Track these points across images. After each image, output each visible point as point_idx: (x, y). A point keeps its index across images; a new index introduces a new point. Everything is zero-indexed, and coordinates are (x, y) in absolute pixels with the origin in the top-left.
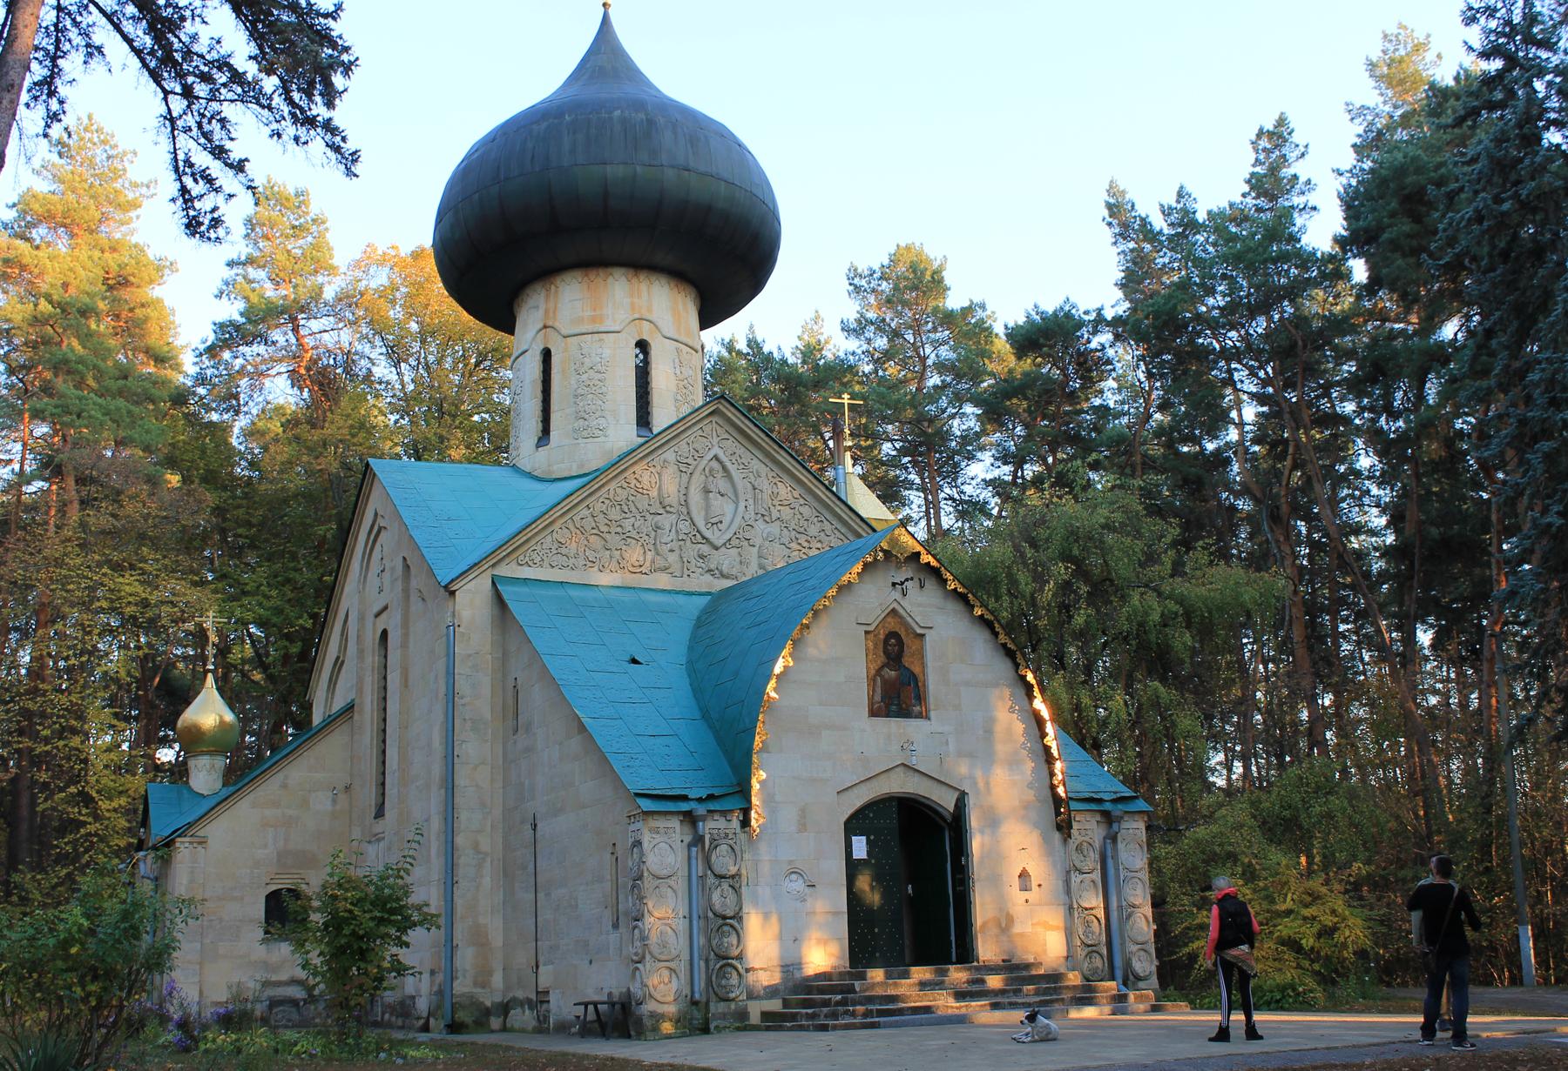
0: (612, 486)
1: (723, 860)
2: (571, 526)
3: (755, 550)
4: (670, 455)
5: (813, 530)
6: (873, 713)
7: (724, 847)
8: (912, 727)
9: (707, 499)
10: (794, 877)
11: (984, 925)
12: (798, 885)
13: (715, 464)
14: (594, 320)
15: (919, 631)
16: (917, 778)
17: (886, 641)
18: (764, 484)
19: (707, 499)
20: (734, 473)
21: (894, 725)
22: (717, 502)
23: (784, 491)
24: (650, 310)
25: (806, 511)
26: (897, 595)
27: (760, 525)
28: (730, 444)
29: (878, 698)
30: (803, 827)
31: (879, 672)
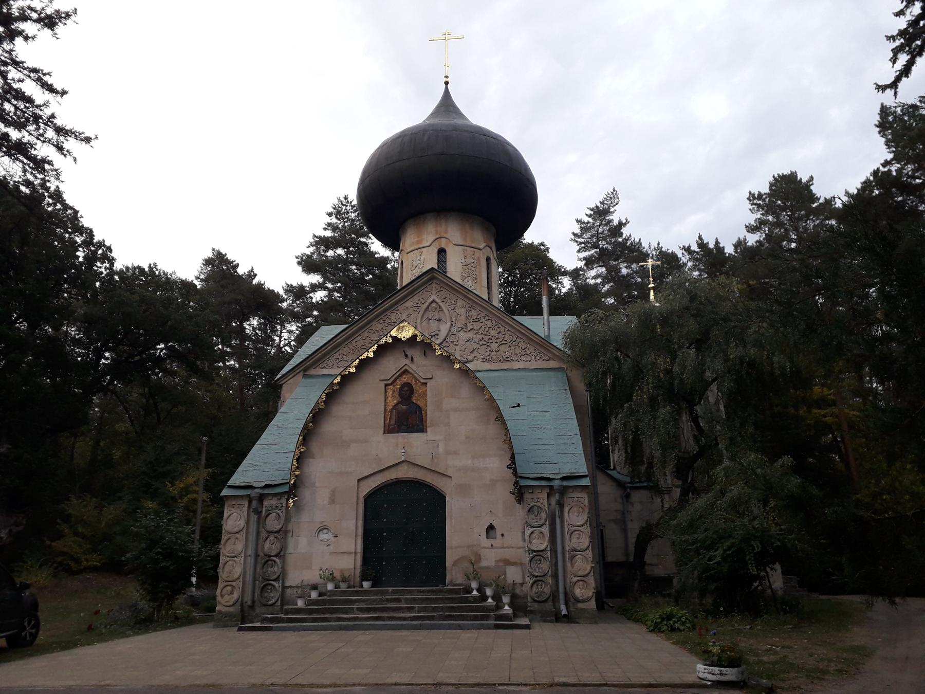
0: (375, 322)
1: (273, 523)
2: (351, 347)
3: (457, 348)
4: (409, 304)
5: (493, 333)
6: (388, 430)
7: (273, 515)
8: (416, 439)
9: (428, 324)
10: (325, 531)
11: (455, 563)
12: (324, 536)
13: (434, 305)
14: (418, 242)
15: (422, 381)
16: (416, 469)
17: (401, 389)
18: (463, 311)
19: (428, 324)
20: (444, 308)
21: (401, 438)
22: (434, 325)
23: (474, 313)
24: (446, 232)
25: (489, 323)
26: (407, 362)
27: (462, 334)
28: (444, 293)
29: (393, 422)
30: (332, 501)
31: (395, 407)
